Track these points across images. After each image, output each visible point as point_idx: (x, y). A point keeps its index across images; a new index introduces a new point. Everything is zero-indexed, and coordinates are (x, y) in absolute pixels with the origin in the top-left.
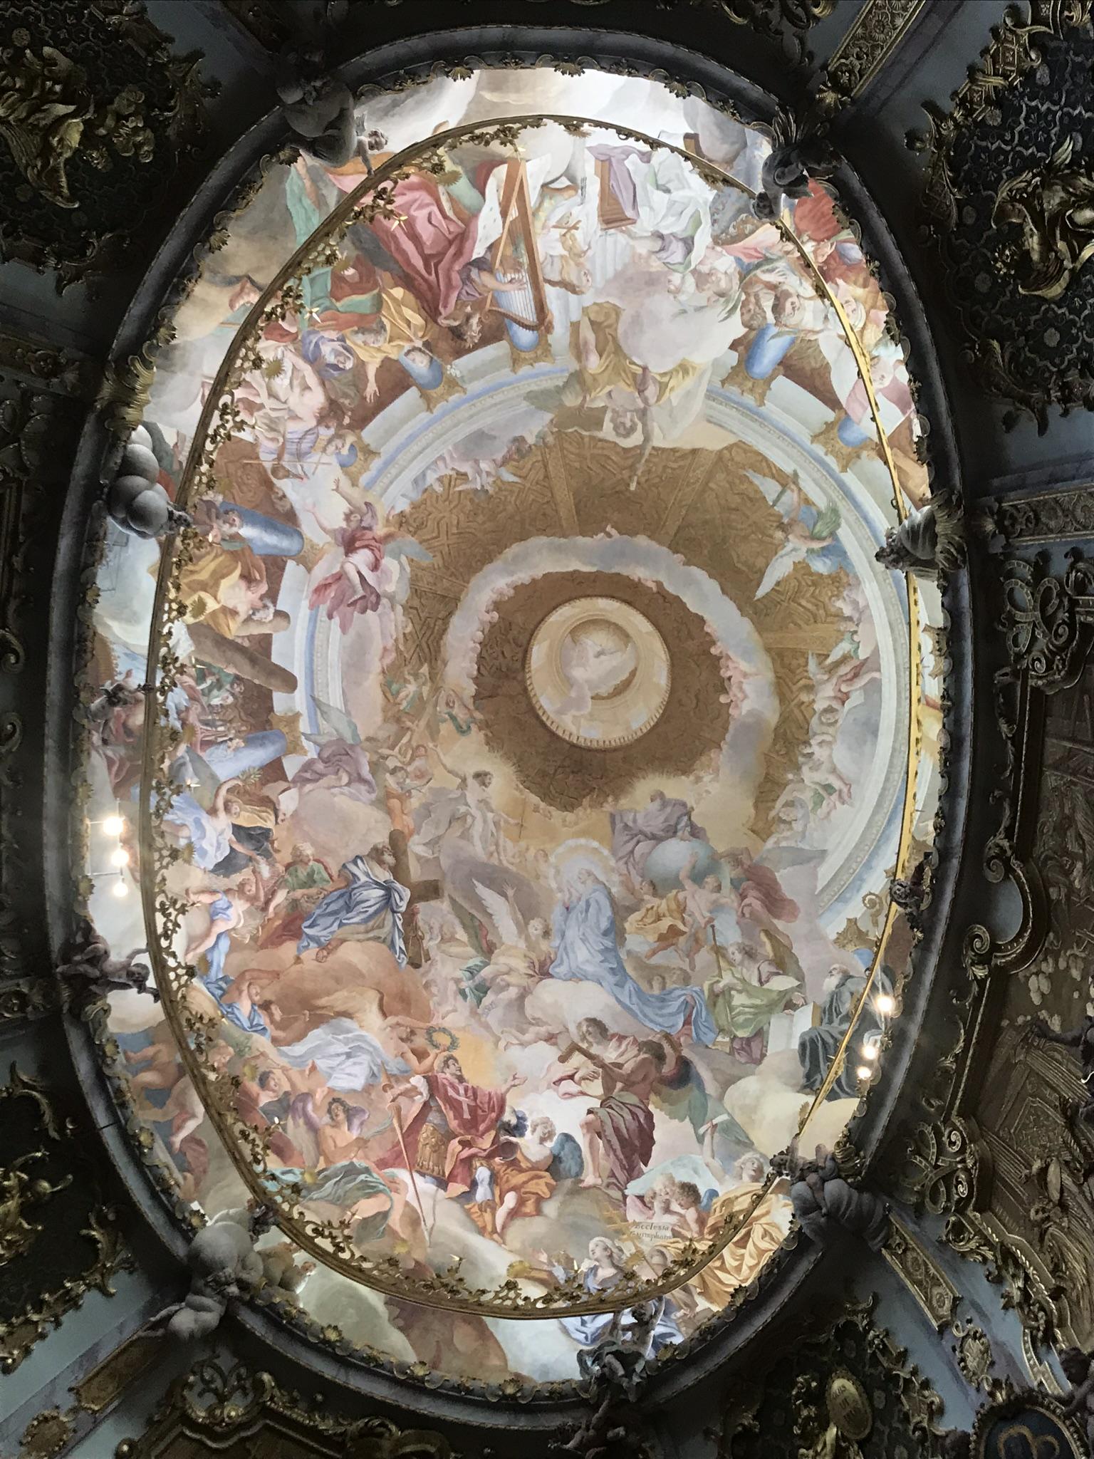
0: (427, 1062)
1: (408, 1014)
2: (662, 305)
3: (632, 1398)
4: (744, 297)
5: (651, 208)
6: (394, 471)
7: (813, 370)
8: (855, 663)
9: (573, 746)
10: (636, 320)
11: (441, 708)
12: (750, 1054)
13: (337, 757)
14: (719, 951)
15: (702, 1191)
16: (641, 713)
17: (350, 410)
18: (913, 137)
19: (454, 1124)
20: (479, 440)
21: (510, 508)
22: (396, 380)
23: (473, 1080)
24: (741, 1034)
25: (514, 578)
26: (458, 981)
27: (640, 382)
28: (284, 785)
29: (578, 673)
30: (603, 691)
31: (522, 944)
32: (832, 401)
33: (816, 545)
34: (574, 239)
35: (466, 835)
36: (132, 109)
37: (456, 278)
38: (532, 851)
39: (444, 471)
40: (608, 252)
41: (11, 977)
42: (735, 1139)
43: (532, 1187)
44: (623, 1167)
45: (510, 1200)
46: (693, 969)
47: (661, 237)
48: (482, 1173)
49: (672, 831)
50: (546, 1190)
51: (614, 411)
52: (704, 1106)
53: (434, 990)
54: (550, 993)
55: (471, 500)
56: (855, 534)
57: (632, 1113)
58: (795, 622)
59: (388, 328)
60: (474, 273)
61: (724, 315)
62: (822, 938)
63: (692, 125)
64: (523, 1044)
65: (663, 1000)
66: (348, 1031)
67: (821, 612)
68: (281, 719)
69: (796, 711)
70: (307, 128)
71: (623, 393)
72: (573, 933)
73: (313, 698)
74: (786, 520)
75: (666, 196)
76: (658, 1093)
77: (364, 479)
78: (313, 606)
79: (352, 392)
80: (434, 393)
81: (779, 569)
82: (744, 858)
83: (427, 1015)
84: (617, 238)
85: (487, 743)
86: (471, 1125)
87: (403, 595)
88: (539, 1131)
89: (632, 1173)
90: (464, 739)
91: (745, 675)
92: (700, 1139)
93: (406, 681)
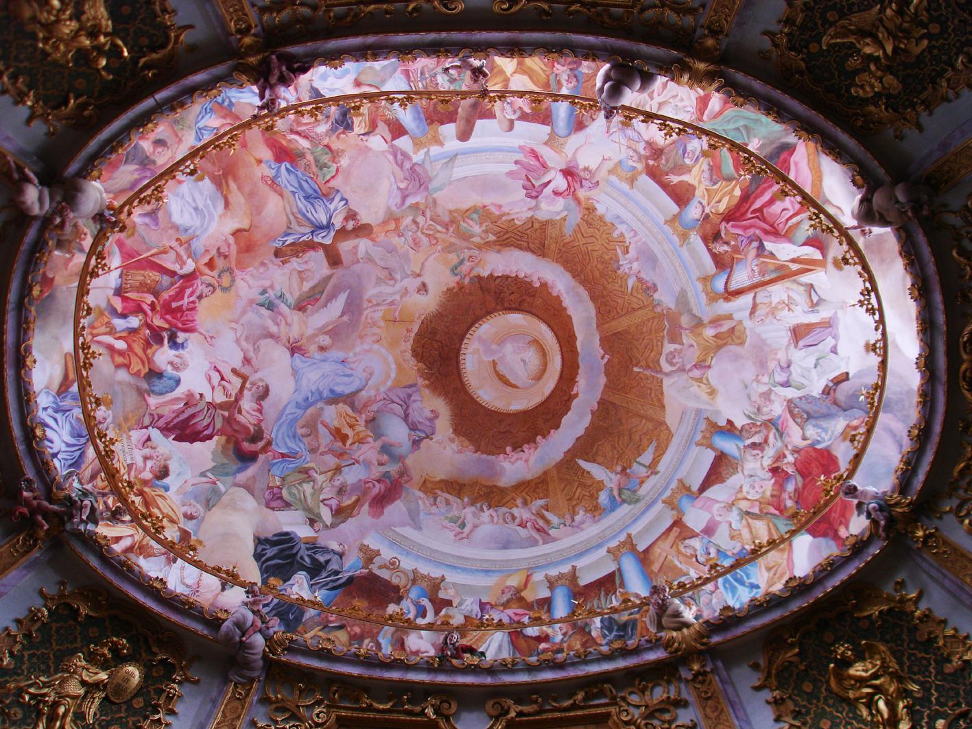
0: (206, 270)
1: (240, 252)
2: (749, 372)
3: (68, 527)
4: (759, 423)
5: (804, 358)
6: (622, 200)
7: (720, 473)
8: (546, 528)
9: (459, 350)
10: (737, 357)
11: (467, 253)
12: (272, 500)
13: (417, 178)
14: (338, 470)
15: (166, 481)
16: (488, 395)
17: (656, 166)
18: (902, 584)
19: (165, 296)
20: (652, 260)
21: (610, 286)
22: (681, 196)
23: (202, 306)
24: (285, 493)
25: (565, 295)
26: (272, 287)
27: (701, 365)
28: (389, 137)
29: (509, 348)
30: (500, 368)
31: (310, 332)
32: (704, 487)
33: (615, 493)
34: (783, 309)
35: (379, 281)
36: (887, 86)
37: (751, 231)
38: (378, 331)
39: (628, 236)
40: (776, 333)
41: (261, 20)
42: (211, 500)
43: (134, 360)
44: (167, 424)
45: (121, 345)
46: (321, 454)
47: (789, 366)
48: (134, 322)
49: (413, 427)
50: (136, 370)
51: (681, 350)
52: (227, 474)
53: (262, 269)
54: (280, 355)
55: (611, 258)
56: (626, 514)
57: (209, 425)
58: (565, 488)
59: (716, 187)
60: (755, 244)
61: (747, 413)
62: (363, 535)
63: (854, 377)
64: (237, 341)
65: (294, 436)
66: (215, 207)
67: (575, 503)
68: (436, 132)
69: (508, 498)
70: (877, 199)
71: (692, 356)
72: (327, 368)
73: (456, 155)
74: (628, 471)
75: (813, 366)
76: (228, 441)
77: (613, 178)
78: (521, 148)
79: (670, 165)
80: (677, 224)
81: (597, 471)
82: (405, 478)
83: (241, 266)
84: (786, 337)
85: (448, 289)
86: (168, 310)
87: (542, 215)
88: (177, 360)
89: (166, 430)
90: (448, 272)
91: (526, 461)
92: (203, 474)
93: (481, 224)
